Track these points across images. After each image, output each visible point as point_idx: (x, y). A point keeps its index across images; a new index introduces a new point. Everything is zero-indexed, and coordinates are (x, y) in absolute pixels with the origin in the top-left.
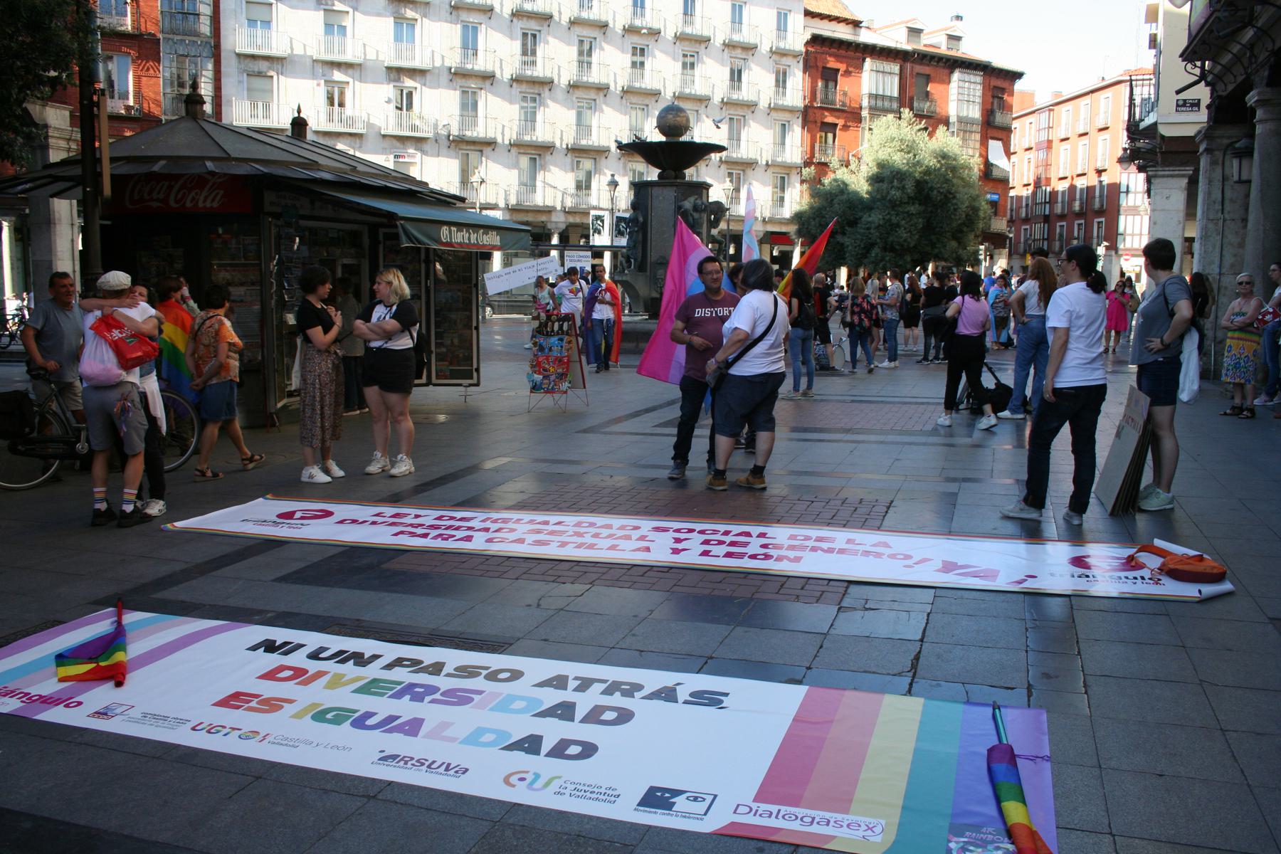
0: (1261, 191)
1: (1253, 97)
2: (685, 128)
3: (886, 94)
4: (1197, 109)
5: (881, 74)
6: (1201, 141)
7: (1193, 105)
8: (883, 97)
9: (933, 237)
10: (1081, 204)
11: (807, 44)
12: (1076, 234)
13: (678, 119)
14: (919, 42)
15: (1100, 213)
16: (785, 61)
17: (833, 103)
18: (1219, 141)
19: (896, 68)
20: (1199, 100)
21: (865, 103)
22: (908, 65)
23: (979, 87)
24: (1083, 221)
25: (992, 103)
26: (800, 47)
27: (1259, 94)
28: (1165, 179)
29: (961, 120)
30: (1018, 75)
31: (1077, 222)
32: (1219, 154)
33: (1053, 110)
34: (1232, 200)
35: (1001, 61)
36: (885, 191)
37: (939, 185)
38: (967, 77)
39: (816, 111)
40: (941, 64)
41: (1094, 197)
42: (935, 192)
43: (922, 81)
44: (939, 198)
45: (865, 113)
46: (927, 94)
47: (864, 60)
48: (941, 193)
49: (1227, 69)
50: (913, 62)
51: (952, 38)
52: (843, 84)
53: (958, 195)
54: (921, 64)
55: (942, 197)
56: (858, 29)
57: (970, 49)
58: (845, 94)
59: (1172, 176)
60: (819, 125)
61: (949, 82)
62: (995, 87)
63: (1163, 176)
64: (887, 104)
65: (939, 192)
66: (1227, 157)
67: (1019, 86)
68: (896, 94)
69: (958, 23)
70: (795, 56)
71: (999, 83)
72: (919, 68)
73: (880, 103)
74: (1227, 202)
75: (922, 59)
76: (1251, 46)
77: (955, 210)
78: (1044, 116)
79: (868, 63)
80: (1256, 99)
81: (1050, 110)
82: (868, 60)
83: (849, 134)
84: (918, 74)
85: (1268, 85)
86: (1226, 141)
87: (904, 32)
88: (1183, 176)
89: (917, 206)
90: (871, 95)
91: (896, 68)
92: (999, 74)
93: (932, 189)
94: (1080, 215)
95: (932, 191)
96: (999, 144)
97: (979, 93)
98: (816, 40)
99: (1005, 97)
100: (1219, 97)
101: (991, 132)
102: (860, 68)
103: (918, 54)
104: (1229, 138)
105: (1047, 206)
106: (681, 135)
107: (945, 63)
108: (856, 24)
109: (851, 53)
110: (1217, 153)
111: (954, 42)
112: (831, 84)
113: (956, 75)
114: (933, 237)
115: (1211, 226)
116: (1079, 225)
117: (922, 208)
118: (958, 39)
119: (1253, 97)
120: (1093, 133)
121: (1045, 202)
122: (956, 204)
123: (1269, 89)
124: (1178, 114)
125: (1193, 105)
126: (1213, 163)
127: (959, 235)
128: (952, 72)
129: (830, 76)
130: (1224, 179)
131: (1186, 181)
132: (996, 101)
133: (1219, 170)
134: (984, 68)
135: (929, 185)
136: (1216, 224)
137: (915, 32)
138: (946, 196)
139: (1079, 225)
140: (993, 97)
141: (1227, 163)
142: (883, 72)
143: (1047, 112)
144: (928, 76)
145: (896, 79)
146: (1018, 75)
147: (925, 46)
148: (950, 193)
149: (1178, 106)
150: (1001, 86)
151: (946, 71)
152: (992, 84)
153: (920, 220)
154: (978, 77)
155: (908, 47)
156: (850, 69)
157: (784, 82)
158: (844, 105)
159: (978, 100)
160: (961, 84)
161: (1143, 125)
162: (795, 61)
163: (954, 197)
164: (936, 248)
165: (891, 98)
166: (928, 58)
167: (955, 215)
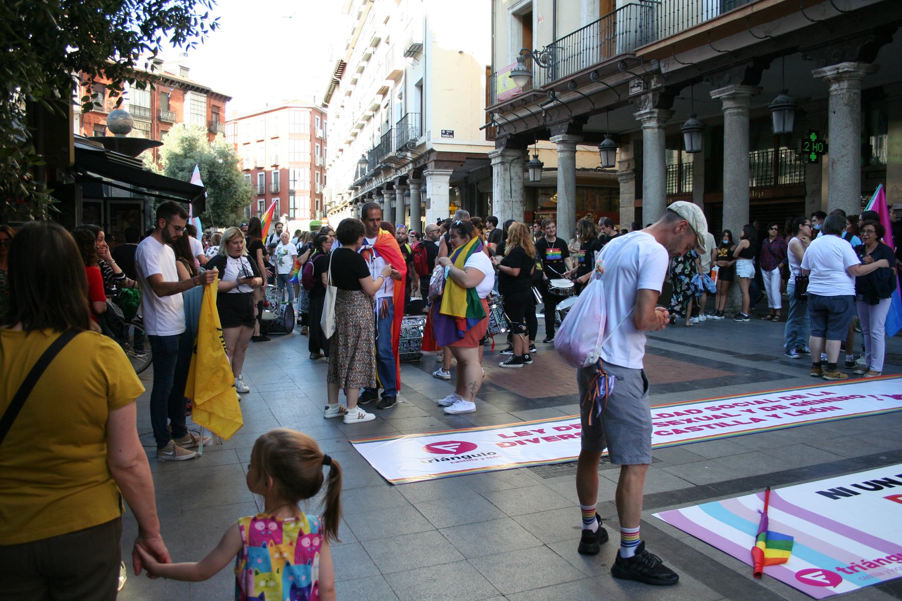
0: (565, 187)
1: (558, 138)
2: (127, 129)
3: (141, 106)
4: (452, 136)
6: (495, 157)
7: (450, 134)
8: (140, 108)
9: (219, 211)
10: (261, 188)
12: (259, 209)
13: (127, 121)
14: (161, 70)
15: (276, 194)
18: (507, 158)
20: (453, 131)
23: (204, 105)
24: (263, 200)
25: (212, 116)
27: (563, 137)
28: (438, 176)
30: (227, 99)
31: (259, 200)
32: (507, 165)
33: (236, 123)
34: (515, 191)
35: (215, 89)
36: (188, 178)
37: (224, 174)
41: (271, 184)
42: (221, 179)
44: (224, 183)
46: (169, 107)
48: (226, 180)
49: (521, 119)
50: (158, 84)
53: (237, 182)
54: (164, 86)
55: (227, 183)
57: (191, 78)
59: (441, 175)
60: (93, 125)
61: (184, 100)
62: (213, 106)
63: (436, 175)
64: (142, 113)
65: (224, 179)
66: (512, 167)
67: (228, 104)
68: (148, 106)
69: (185, 58)
71: (216, 103)
73: (137, 112)
74: (513, 192)
75: (165, 82)
76: (547, 110)
77: (235, 192)
80: (561, 139)
81: (235, 123)
84: (162, 92)
85: (567, 133)
86: (511, 158)
88: (447, 175)
89: (210, 189)
92: (212, 96)
93: (218, 177)
94: (261, 195)
95: (219, 178)
97: (205, 109)
99: (220, 113)
100: (510, 134)
103: (163, 78)
104: (512, 156)
106: (127, 133)
107: (181, 86)
110: (507, 164)
111: (184, 72)
113: (189, 95)
114: (219, 211)
115: (506, 205)
116: (260, 202)
117: (212, 190)
118: (187, 69)
119: (558, 138)
120: (268, 140)
122: (236, 188)
123: (567, 135)
124: (443, 139)
125: (450, 134)
126: (505, 170)
127: (235, 209)
128: (185, 93)
130: (511, 179)
131: (449, 177)
132: (214, 116)
133: (508, 173)
135: (217, 174)
136: (509, 204)
138: (228, 182)
139: (260, 202)
141: (512, 170)
143: (233, 125)
146: (227, 99)
147: (165, 72)
148: (232, 180)
149: (442, 134)
150: (217, 105)
151: (181, 92)
152: (212, 103)
153: (212, 199)
154: (203, 98)
159: (205, 114)
161: (418, 144)
163: (234, 183)
164: (222, 218)
165: (145, 109)
166: (170, 81)
167: (235, 195)
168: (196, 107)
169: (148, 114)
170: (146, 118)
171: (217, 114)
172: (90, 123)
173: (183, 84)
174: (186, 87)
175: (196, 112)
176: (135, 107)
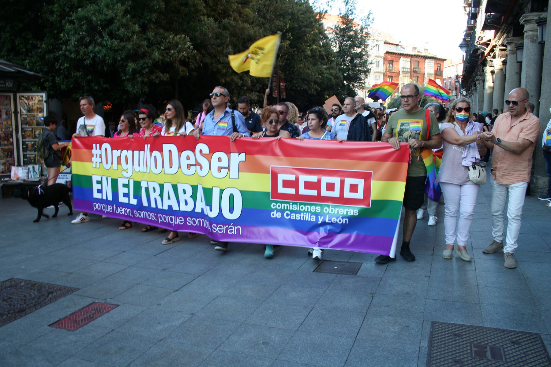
5: (405, 62)
8: (406, 68)
11: (384, 54)
16: (379, 59)
17: (392, 70)
19: (409, 60)
21: (401, 70)
22: (413, 59)
23: (433, 64)
26: (383, 55)
29: (428, 74)
35: (439, 56)
38: (430, 61)
40: (422, 58)
43: (417, 63)
45: (401, 73)
47: (400, 57)
51: (425, 49)
56: (398, 46)
58: (395, 68)
61: (425, 63)
62: (438, 64)
64: (407, 70)
68: (409, 67)
70: (381, 57)
71: (439, 62)
72: (416, 59)
73: (405, 70)
78: (455, 67)
79: (402, 59)
82: (402, 58)
84: (416, 61)
90: (402, 68)
91: (409, 60)
96: (440, 80)
97: (433, 66)
98: (387, 53)
101: (437, 77)
105: (456, 97)
108: (397, 45)
109: (396, 56)
111: (426, 51)
113: (427, 60)
118: (427, 50)
121: (455, 95)
128: (426, 60)
129: (391, 62)
134: (435, 58)
137: (415, 48)
140: (438, 66)
142: (406, 61)
144: (418, 61)
151: (424, 60)
154: (433, 61)
157: (378, 65)
158: (395, 70)
160: (428, 63)
165: (408, 68)
168: (430, 65)
169: (409, 70)
170: (408, 72)
171: (440, 67)
172: (387, 76)
173: (424, 57)
174: (426, 58)
175: (430, 67)
176: (404, 68)
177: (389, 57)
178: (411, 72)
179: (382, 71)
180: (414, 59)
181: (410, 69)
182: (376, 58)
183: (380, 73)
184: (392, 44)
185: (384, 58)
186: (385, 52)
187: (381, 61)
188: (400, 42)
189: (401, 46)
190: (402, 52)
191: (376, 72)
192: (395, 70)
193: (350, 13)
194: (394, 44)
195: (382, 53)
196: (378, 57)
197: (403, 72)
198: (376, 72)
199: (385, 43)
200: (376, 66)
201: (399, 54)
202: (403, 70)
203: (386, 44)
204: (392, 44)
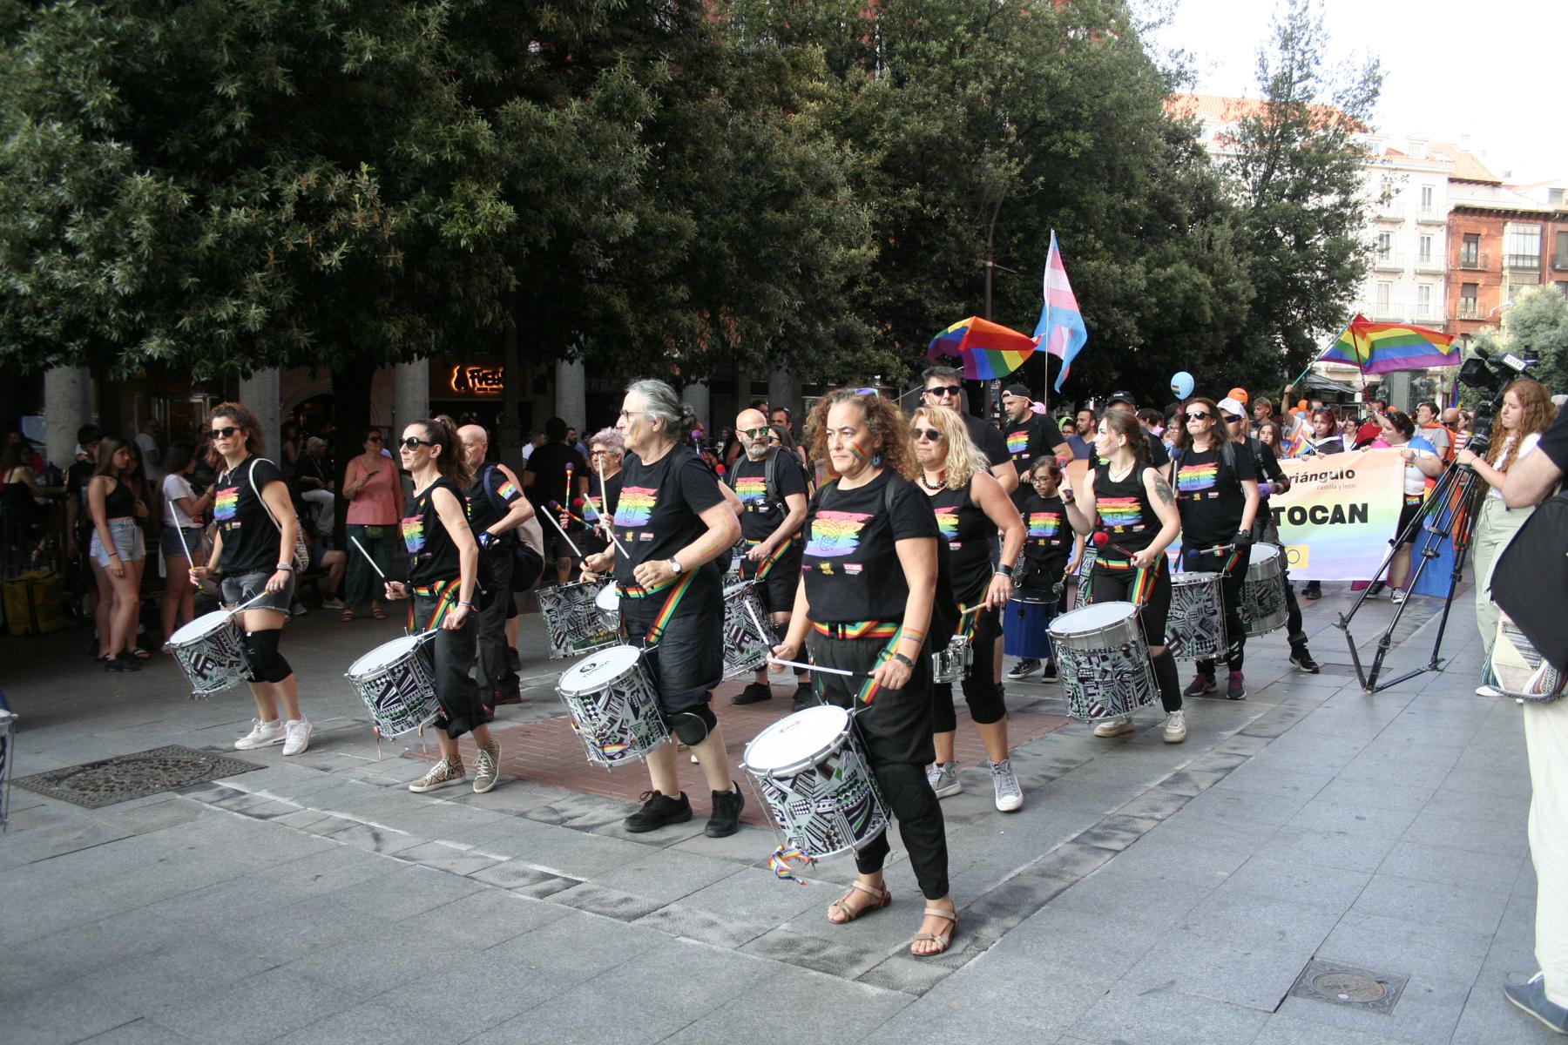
8: (1524, 257)
11: (1451, 213)
16: (1429, 230)
19: (1537, 229)
21: (1506, 263)
22: (1550, 225)
26: (1443, 217)
39: (1459, 274)
45: (1506, 273)
47: (1505, 223)
50: (1555, 221)
52: (1486, 249)
56: (1497, 190)
58: (1486, 256)
64: (1528, 263)
68: (1536, 252)
70: (1439, 226)
73: (1520, 263)
79: (1510, 227)
82: (1509, 224)
83: (1490, 293)
87: (1546, 193)
90: (1511, 256)
98: (1460, 210)
102: (1502, 234)
108: (1496, 185)
112: (1473, 246)
137: (1557, 193)
145: (1537, 239)
155: (1549, 208)
156: (1493, 232)
162: (1439, 230)
165: (1532, 257)
169: (1535, 263)
170: (1532, 268)
176: (1517, 257)
177: (1469, 224)
178: (1541, 268)
179: (1443, 269)
180: (1553, 229)
181: (1540, 257)
182: (1423, 228)
183: (1435, 274)
184: (1477, 182)
185: (1449, 228)
186: (1452, 208)
187: (1439, 238)
188: (1509, 175)
189: (1509, 187)
190: (1511, 207)
191: (1422, 274)
192: (1485, 266)
193: (1296, 75)
194: (1486, 183)
195: (1441, 211)
196: (1428, 224)
197: (1512, 268)
198: (1422, 274)
199: (1452, 180)
200: (1422, 254)
201: (1499, 211)
202: (1513, 263)
203: (1457, 186)
204: (1477, 182)
